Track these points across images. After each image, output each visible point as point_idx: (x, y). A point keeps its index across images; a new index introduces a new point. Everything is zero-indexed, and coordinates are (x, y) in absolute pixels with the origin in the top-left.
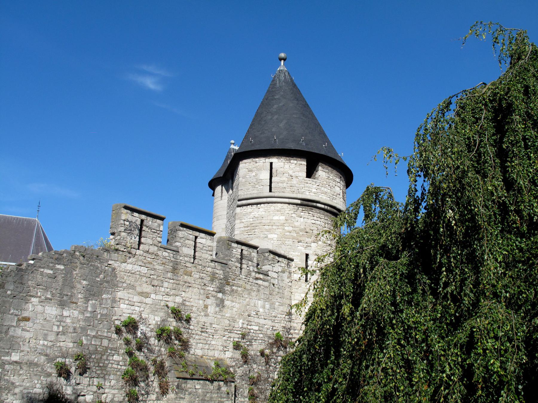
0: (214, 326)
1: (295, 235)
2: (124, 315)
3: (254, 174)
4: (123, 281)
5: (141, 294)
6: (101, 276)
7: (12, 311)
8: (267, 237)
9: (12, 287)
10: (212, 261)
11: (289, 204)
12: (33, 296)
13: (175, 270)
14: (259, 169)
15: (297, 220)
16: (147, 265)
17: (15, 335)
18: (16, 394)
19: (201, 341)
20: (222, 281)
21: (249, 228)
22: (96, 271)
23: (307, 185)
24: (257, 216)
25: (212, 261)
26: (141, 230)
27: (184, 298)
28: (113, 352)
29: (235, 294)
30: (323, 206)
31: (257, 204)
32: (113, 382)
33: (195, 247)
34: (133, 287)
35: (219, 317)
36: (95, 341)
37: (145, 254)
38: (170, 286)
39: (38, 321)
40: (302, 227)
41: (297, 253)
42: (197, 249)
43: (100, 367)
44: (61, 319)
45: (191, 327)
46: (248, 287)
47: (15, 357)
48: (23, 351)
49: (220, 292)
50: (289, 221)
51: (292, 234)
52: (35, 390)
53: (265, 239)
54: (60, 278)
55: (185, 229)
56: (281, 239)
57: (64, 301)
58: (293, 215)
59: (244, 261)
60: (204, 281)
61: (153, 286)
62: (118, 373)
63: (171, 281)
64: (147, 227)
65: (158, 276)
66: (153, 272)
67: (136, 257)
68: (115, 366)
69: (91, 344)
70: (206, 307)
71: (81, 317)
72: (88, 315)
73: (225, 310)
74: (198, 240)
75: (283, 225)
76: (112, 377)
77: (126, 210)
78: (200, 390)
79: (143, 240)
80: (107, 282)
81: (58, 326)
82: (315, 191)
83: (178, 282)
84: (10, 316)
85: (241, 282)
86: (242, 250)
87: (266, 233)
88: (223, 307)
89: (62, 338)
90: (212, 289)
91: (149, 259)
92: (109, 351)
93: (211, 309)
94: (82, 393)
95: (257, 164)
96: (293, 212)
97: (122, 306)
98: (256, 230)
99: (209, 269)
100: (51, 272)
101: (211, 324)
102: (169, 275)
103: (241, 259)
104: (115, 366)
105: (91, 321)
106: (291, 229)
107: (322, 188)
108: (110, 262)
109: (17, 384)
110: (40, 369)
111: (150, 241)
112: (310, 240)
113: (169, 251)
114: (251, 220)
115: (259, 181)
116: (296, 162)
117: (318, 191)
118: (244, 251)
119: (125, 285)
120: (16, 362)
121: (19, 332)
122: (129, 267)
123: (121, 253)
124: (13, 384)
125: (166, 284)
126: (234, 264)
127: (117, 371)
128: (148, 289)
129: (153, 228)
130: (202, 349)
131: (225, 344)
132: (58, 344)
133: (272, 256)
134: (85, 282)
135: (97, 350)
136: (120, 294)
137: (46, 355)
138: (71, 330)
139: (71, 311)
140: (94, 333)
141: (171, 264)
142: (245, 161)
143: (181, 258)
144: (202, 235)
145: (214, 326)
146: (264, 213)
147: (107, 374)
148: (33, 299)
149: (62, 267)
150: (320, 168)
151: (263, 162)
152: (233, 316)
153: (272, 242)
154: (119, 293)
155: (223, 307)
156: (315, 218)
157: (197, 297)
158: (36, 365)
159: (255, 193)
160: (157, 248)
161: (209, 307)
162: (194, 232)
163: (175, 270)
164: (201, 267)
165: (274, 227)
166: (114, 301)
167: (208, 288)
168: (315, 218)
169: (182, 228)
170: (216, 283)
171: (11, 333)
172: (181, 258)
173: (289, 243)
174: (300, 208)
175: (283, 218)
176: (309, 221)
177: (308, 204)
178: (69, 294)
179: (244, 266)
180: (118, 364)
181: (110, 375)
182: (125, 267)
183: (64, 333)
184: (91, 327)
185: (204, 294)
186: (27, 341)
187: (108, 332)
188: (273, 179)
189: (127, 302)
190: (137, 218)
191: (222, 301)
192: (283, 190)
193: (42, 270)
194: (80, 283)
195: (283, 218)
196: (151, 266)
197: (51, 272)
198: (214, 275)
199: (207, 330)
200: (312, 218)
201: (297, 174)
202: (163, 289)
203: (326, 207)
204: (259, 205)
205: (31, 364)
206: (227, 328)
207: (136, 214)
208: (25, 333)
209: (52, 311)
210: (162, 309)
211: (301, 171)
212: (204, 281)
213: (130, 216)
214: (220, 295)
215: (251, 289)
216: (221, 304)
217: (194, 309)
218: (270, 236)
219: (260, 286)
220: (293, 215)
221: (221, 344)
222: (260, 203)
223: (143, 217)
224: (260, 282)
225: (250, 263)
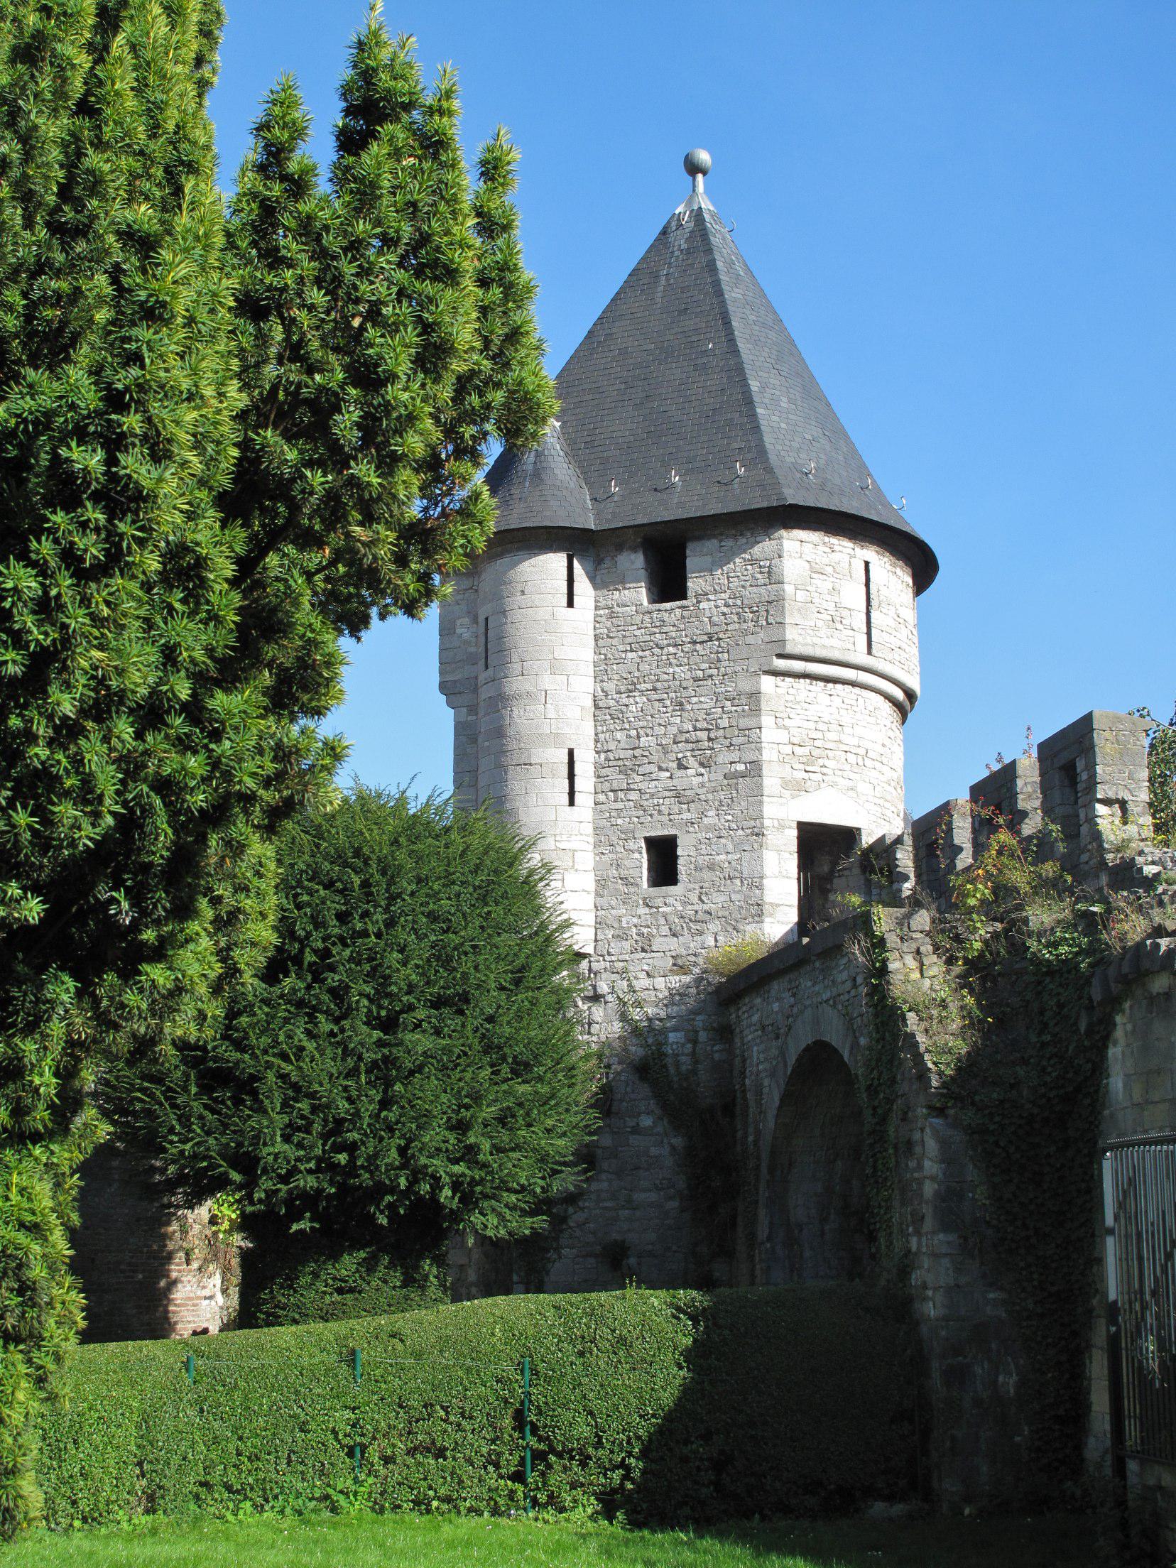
53: (851, 793)
98: (827, 763)
114: (812, 725)
151: (848, 554)
188: (874, 614)
204: (830, 685)
222: (835, 681)
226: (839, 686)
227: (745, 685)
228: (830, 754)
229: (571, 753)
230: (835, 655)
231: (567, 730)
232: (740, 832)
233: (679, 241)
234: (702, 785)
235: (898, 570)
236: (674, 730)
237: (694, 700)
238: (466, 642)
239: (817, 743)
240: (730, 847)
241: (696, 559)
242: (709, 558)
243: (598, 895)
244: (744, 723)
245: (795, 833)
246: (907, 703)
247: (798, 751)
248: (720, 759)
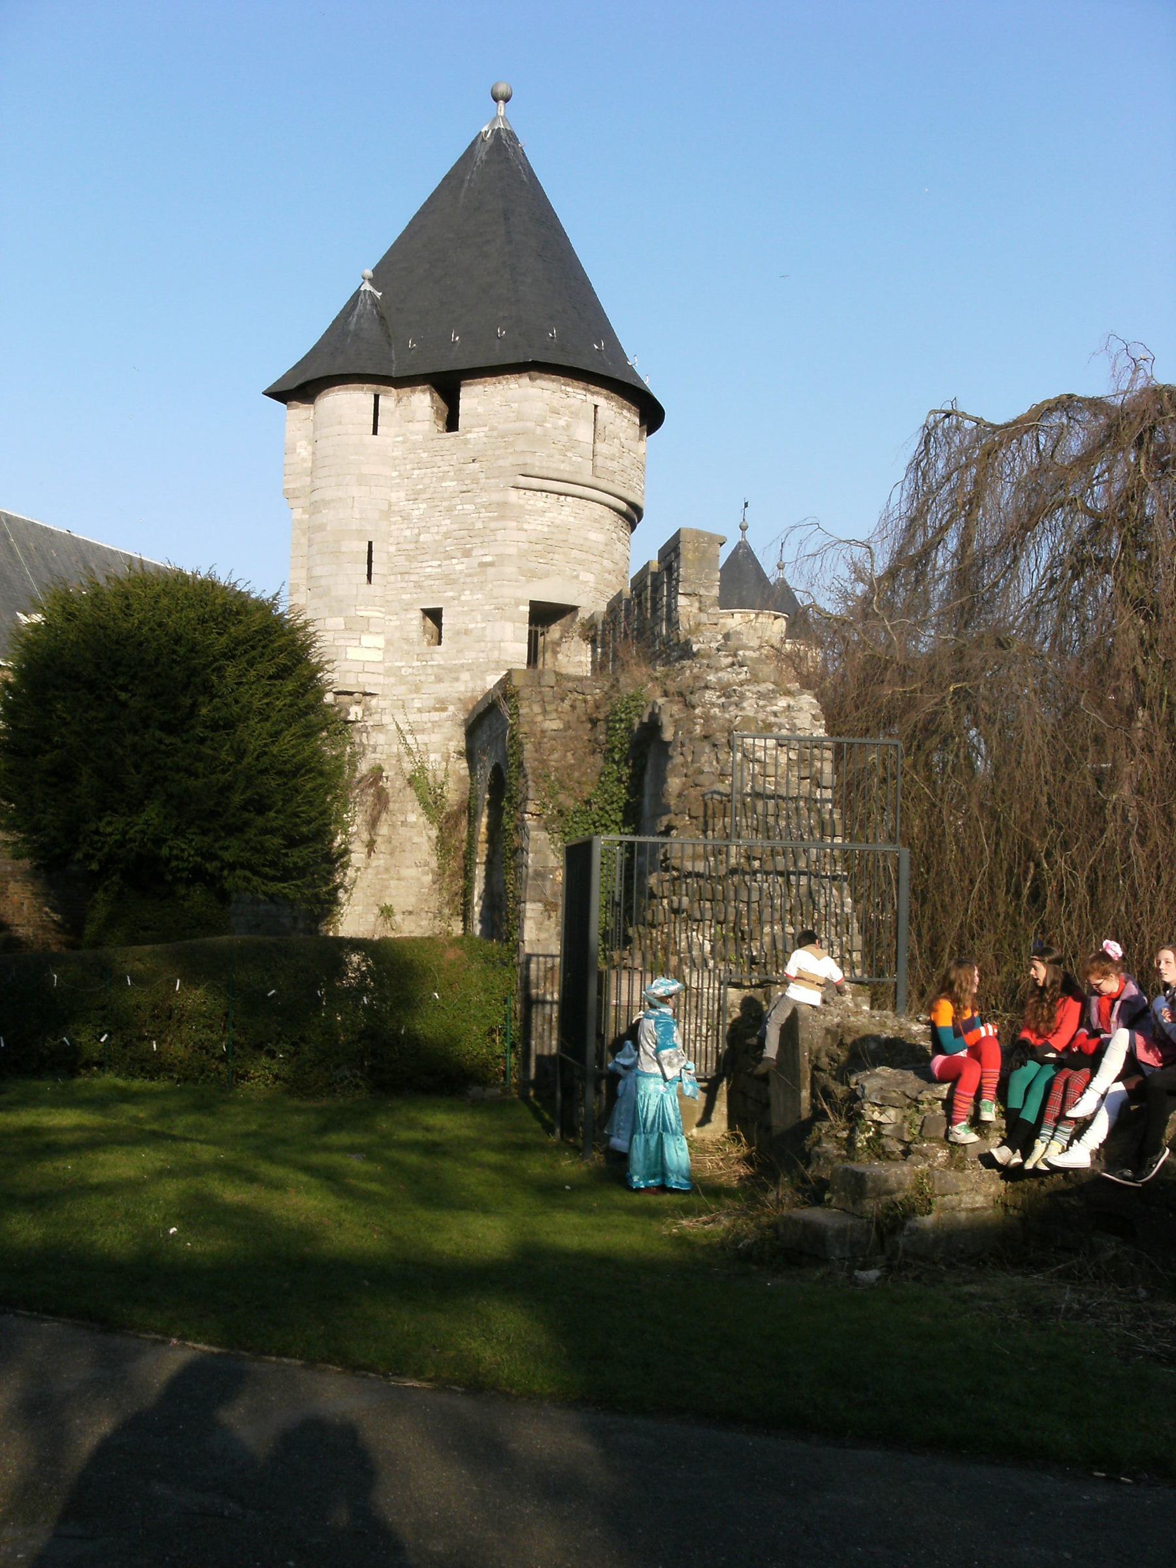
3: (562, 423)
8: (577, 577)
11: (610, 507)
24: (557, 522)
87: (578, 567)
95: (571, 401)
98: (556, 556)
114: (546, 529)
146: (572, 519)
159: (564, 469)
188: (598, 445)
204: (562, 498)
226: (569, 498)
227: (496, 497)
229: (370, 544)
230: (565, 477)
231: (368, 528)
232: (487, 607)
233: (481, 154)
234: (461, 572)
235: (625, 412)
236: (443, 529)
237: (460, 507)
238: (304, 460)
239: (549, 542)
240: (479, 618)
241: (467, 401)
242: (476, 400)
243: (386, 651)
244: (493, 525)
245: (527, 609)
246: (631, 512)
248: (474, 553)
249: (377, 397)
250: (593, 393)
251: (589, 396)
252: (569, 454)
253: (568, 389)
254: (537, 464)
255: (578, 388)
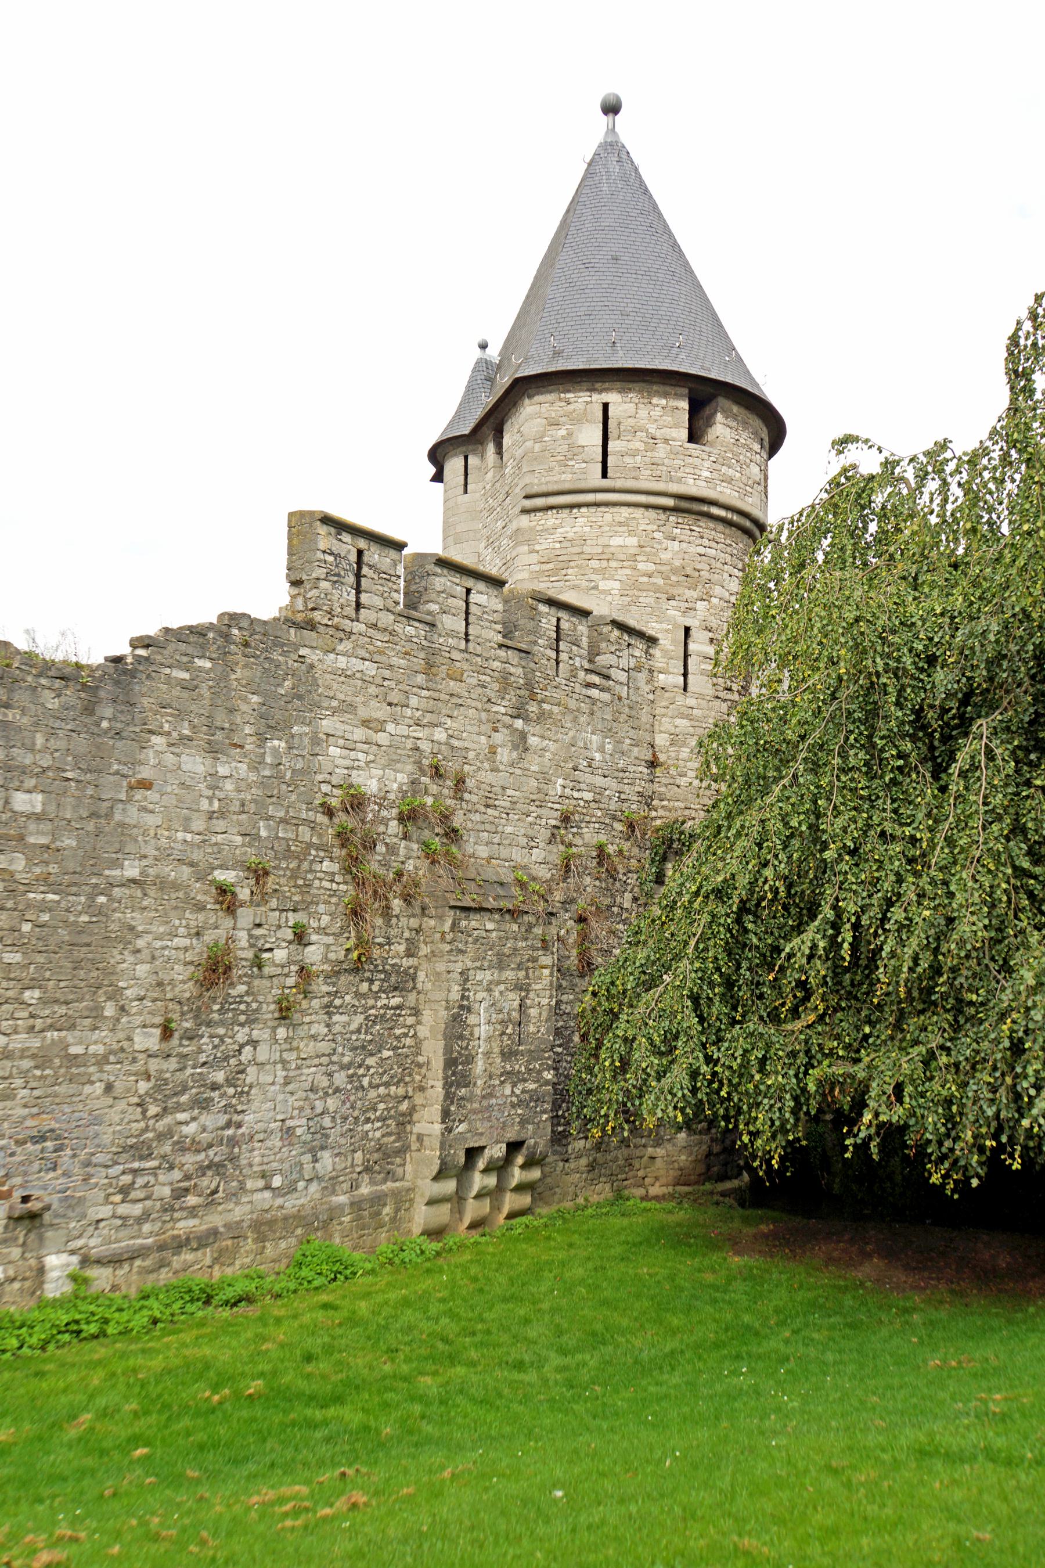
0: (509, 792)
1: (660, 582)
2: (337, 770)
3: (563, 432)
4: (331, 694)
5: (366, 723)
6: (287, 683)
7: (116, 767)
8: (596, 588)
9: (108, 712)
10: (501, 646)
11: (647, 507)
12: (152, 732)
13: (429, 667)
14: (579, 420)
15: (664, 546)
16: (376, 658)
17: (127, 820)
18: (138, 951)
19: (487, 827)
20: (522, 692)
21: (551, 566)
22: (272, 673)
23: (690, 460)
24: (570, 535)
25: (501, 646)
26: (358, 576)
27: (450, 732)
28: (322, 854)
29: (549, 721)
30: (722, 513)
31: (572, 506)
32: (326, 919)
33: (467, 613)
34: (352, 708)
35: (518, 772)
36: (285, 830)
37: (371, 632)
38: (424, 704)
39: (169, 789)
40: (677, 563)
41: (665, 626)
42: (471, 619)
43: (299, 886)
44: (214, 781)
45: (466, 796)
46: (572, 704)
47: (132, 871)
48: (145, 857)
49: (518, 717)
50: (648, 549)
51: (653, 580)
52: (176, 940)
54: (204, 690)
55: (445, 571)
56: (630, 593)
57: (217, 743)
58: (657, 535)
59: (563, 646)
60: (488, 691)
61: (390, 704)
62: (334, 900)
63: (425, 693)
64: (371, 567)
65: (398, 682)
66: (387, 673)
67: (353, 637)
68: (326, 884)
69: (278, 838)
70: (493, 750)
71: (253, 777)
72: (267, 773)
73: (529, 756)
74: (474, 598)
75: (634, 558)
76: (322, 908)
77: (325, 527)
78: (494, 934)
79: (364, 598)
80: (300, 697)
81: (210, 799)
82: (708, 474)
83: (436, 695)
84: (112, 778)
85: (557, 694)
86: (558, 620)
87: (594, 577)
88: (527, 749)
89: (220, 825)
90: (503, 710)
91: (379, 644)
92: (313, 852)
93: (505, 755)
94: (267, 946)
95: (571, 407)
96: (655, 527)
97: (333, 751)
98: (570, 571)
99: (496, 665)
100: (186, 676)
101: (504, 788)
102: (420, 679)
103: (558, 640)
104: (326, 884)
105: (273, 785)
106: (651, 567)
107: (724, 469)
108: (303, 652)
109: (140, 928)
110: (181, 895)
111: (378, 602)
112: (695, 594)
113: (417, 624)
114: (558, 545)
115: (575, 451)
116: (663, 402)
117: (715, 475)
118: (562, 621)
119: (335, 703)
120: (133, 881)
121: (133, 815)
122: (342, 662)
123: (321, 629)
124: (132, 928)
125: (414, 701)
126: (543, 649)
127: (330, 896)
128: (380, 711)
129: (384, 569)
130: (487, 844)
131: (531, 833)
132: (214, 840)
133: (616, 633)
134: (255, 699)
135: (289, 850)
136: (327, 724)
137: (191, 864)
138: (236, 807)
139: (234, 764)
140: (282, 814)
141: (422, 655)
142: (539, 398)
143: (441, 640)
144: (481, 586)
145: (509, 792)
146: (587, 529)
147: (312, 903)
148: (155, 739)
149: (208, 665)
150: (719, 417)
151: (585, 402)
152: (546, 770)
153: (609, 598)
154: (324, 722)
155: (527, 749)
156: (706, 542)
157: (475, 729)
158: (175, 886)
159: (566, 480)
160: (392, 617)
161: (499, 750)
162: (464, 578)
163: (429, 667)
164: (479, 659)
165: (613, 564)
166: (315, 741)
167: (495, 708)
168: (706, 542)
169: (439, 570)
170: (511, 696)
171: (118, 817)
172: (441, 640)
173: (647, 600)
174: (672, 518)
175: (633, 541)
176: (693, 549)
177: (690, 507)
178: (227, 725)
179: (564, 656)
180: (332, 881)
181: (317, 904)
182: (334, 662)
183: (222, 814)
184: (274, 800)
185: (488, 721)
186: (152, 833)
187: (308, 810)
189: (341, 742)
190: (348, 546)
191: (523, 736)
192: (633, 474)
193: (168, 671)
194: (246, 700)
195: (633, 541)
196: (383, 659)
197: (186, 676)
198: (506, 679)
199: (497, 803)
200: (699, 541)
201: (667, 432)
202: (408, 712)
203: (730, 515)
204: (575, 511)
205: (163, 884)
206: (534, 797)
207: (346, 537)
208: (145, 815)
209: (195, 763)
210: (409, 756)
211: (676, 426)
212: (488, 691)
213: (335, 541)
214: (519, 724)
215: (578, 710)
216: (521, 742)
217: (471, 755)
218: (603, 585)
219: (593, 701)
220: (657, 535)
221: (523, 831)
222: (579, 506)
223: (362, 544)
224: (594, 693)
225: (575, 648)
226: (584, 510)
228: (572, 564)
230: (567, 486)
239: (561, 558)
247: (545, 567)
249: (466, 458)
250: (600, 392)
251: (596, 397)
252: (570, 463)
253: (569, 395)
254: (536, 481)
255: (581, 390)
